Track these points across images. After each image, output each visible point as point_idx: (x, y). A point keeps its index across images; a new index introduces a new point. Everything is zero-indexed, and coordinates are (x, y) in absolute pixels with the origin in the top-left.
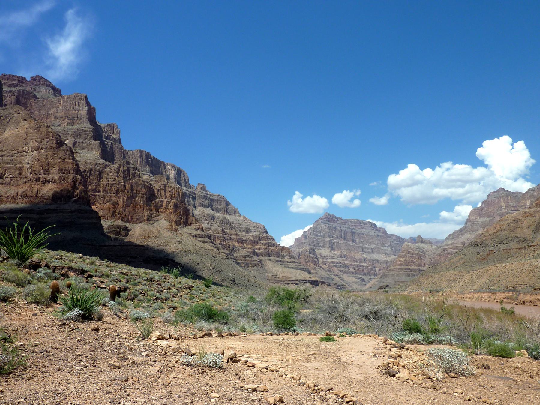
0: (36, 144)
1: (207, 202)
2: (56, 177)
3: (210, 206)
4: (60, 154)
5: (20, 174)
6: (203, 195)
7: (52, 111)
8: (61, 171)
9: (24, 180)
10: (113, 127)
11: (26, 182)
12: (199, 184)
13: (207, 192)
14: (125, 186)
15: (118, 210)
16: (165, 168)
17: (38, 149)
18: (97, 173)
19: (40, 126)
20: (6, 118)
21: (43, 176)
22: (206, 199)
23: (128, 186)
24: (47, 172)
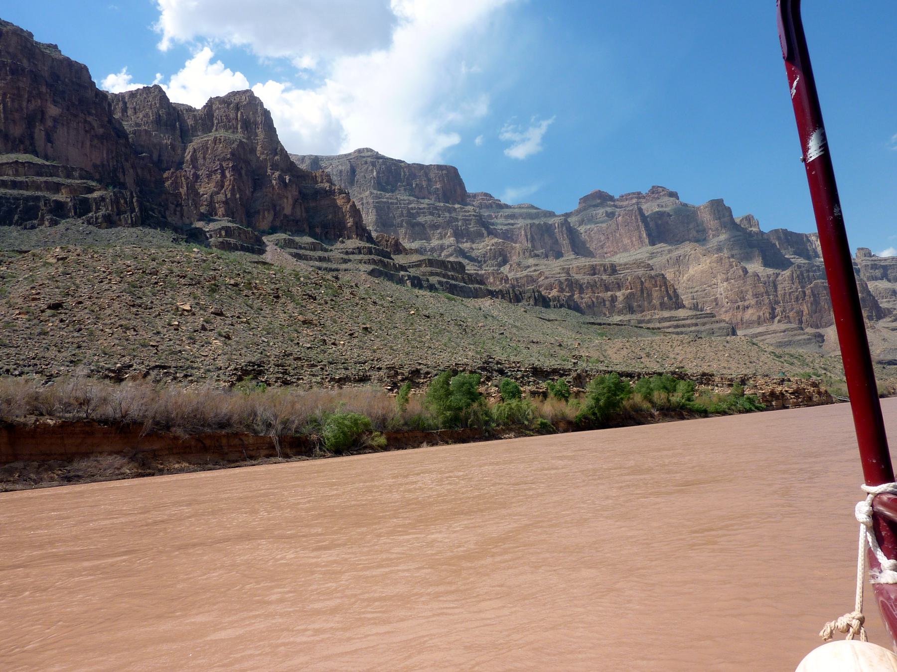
0: (724, 276)
1: (878, 273)
2: (753, 302)
3: (885, 276)
4: (749, 281)
5: (717, 304)
6: (869, 263)
7: (691, 226)
8: (756, 295)
9: (724, 309)
10: (749, 219)
11: (726, 312)
12: (859, 249)
13: (873, 258)
14: (804, 293)
15: (804, 318)
16: (809, 241)
17: (727, 280)
18: (772, 285)
19: (721, 259)
20: (685, 256)
21: (740, 303)
22: (876, 269)
23: (808, 292)
24: (743, 299)
